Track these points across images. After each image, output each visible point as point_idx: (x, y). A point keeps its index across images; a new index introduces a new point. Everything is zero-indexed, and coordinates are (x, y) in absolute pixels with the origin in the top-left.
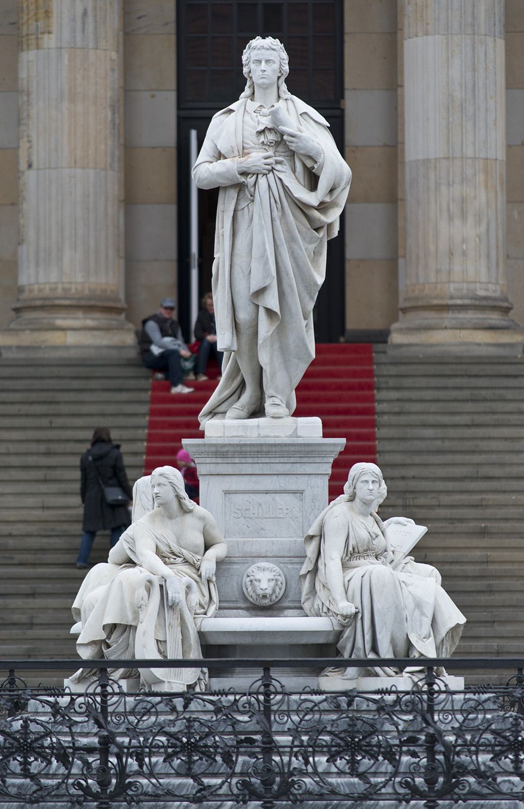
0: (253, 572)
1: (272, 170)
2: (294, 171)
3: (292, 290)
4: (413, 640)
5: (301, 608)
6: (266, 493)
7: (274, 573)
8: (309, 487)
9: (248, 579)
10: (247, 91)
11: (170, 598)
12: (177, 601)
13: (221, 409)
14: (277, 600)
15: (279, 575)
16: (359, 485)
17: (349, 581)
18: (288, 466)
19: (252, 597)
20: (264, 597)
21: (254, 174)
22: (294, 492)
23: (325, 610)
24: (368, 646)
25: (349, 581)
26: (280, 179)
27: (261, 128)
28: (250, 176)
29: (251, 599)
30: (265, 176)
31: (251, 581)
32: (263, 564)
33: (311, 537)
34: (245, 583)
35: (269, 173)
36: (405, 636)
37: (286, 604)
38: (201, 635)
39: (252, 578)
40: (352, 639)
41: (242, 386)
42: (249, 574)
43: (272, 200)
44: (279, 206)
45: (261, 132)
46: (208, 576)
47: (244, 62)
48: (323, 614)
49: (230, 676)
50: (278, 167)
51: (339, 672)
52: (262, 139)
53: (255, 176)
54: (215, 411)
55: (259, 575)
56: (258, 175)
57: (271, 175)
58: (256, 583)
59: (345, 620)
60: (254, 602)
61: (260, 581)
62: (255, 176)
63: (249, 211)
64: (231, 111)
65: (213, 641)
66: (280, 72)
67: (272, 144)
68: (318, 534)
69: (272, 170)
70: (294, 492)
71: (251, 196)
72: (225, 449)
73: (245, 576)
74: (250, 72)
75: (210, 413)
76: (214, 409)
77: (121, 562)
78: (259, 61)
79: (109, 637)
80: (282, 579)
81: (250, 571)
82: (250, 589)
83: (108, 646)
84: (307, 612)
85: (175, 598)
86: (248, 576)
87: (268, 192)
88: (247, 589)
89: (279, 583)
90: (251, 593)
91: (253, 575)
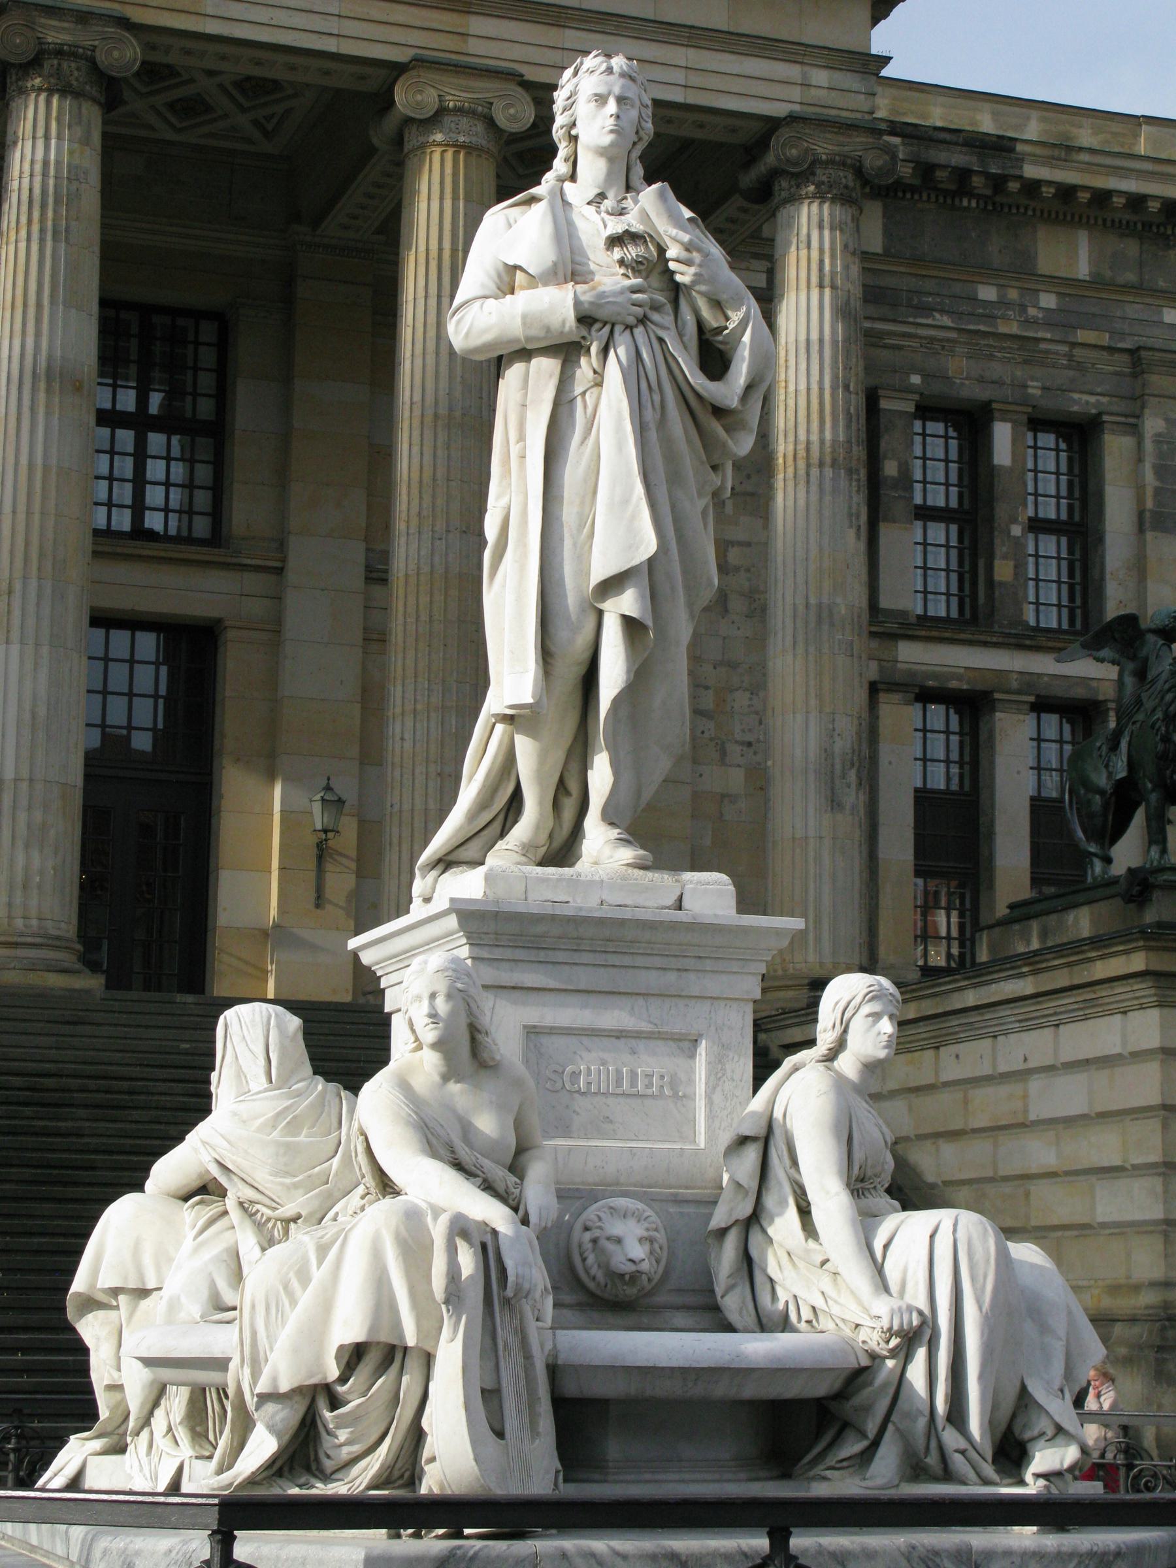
0: (600, 1219)
1: (643, 320)
2: (681, 335)
3: (673, 589)
4: (1038, 1392)
5: (716, 1308)
6: (618, 1038)
7: (646, 1225)
8: (713, 1028)
9: (588, 1236)
10: (560, 165)
11: (511, 1278)
12: (526, 1286)
13: (470, 852)
14: (648, 1287)
15: (656, 1230)
16: (858, 1025)
17: (886, 1247)
18: (672, 977)
19: (594, 1278)
20: (634, 1277)
21: (605, 323)
22: (677, 1039)
23: (806, 1314)
24: (941, 1406)
25: (886, 1247)
26: (661, 340)
27: (620, 229)
28: (597, 326)
29: (591, 1285)
30: (628, 331)
31: (595, 1241)
32: (621, 1202)
33: (743, 1141)
34: (580, 1246)
35: (636, 326)
36: (1018, 1384)
37: (661, 1298)
38: (553, 1370)
39: (597, 1233)
40: (891, 1391)
41: (515, 803)
42: (589, 1224)
43: (644, 385)
44: (657, 398)
45: (615, 241)
46: (543, 1225)
47: (557, 107)
48: (803, 1326)
49: (597, 1476)
50: (655, 317)
51: (851, 1470)
52: (617, 253)
53: (607, 328)
54: (450, 858)
55: (617, 1228)
56: (613, 325)
57: (639, 331)
58: (611, 1247)
59: (888, 1342)
60: (598, 1292)
61: (619, 1241)
62: (607, 328)
63: (585, 407)
64: (534, 199)
65: (571, 1389)
66: (637, 133)
67: (641, 267)
68: (762, 1132)
69: (643, 320)
70: (677, 1039)
71: (595, 372)
72: (540, 929)
73: (578, 1227)
74: (574, 124)
75: (439, 861)
76: (446, 855)
77: (183, 1192)
78: (601, 99)
79: (343, 1380)
80: (661, 1237)
81: (593, 1217)
82: (591, 1259)
83: (335, 1403)
84: (733, 1317)
85: (523, 1277)
86: (587, 1229)
87: (635, 366)
88: (584, 1260)
89: (656, 1246)
90: (594, 1271)
91: (600, 1228)
